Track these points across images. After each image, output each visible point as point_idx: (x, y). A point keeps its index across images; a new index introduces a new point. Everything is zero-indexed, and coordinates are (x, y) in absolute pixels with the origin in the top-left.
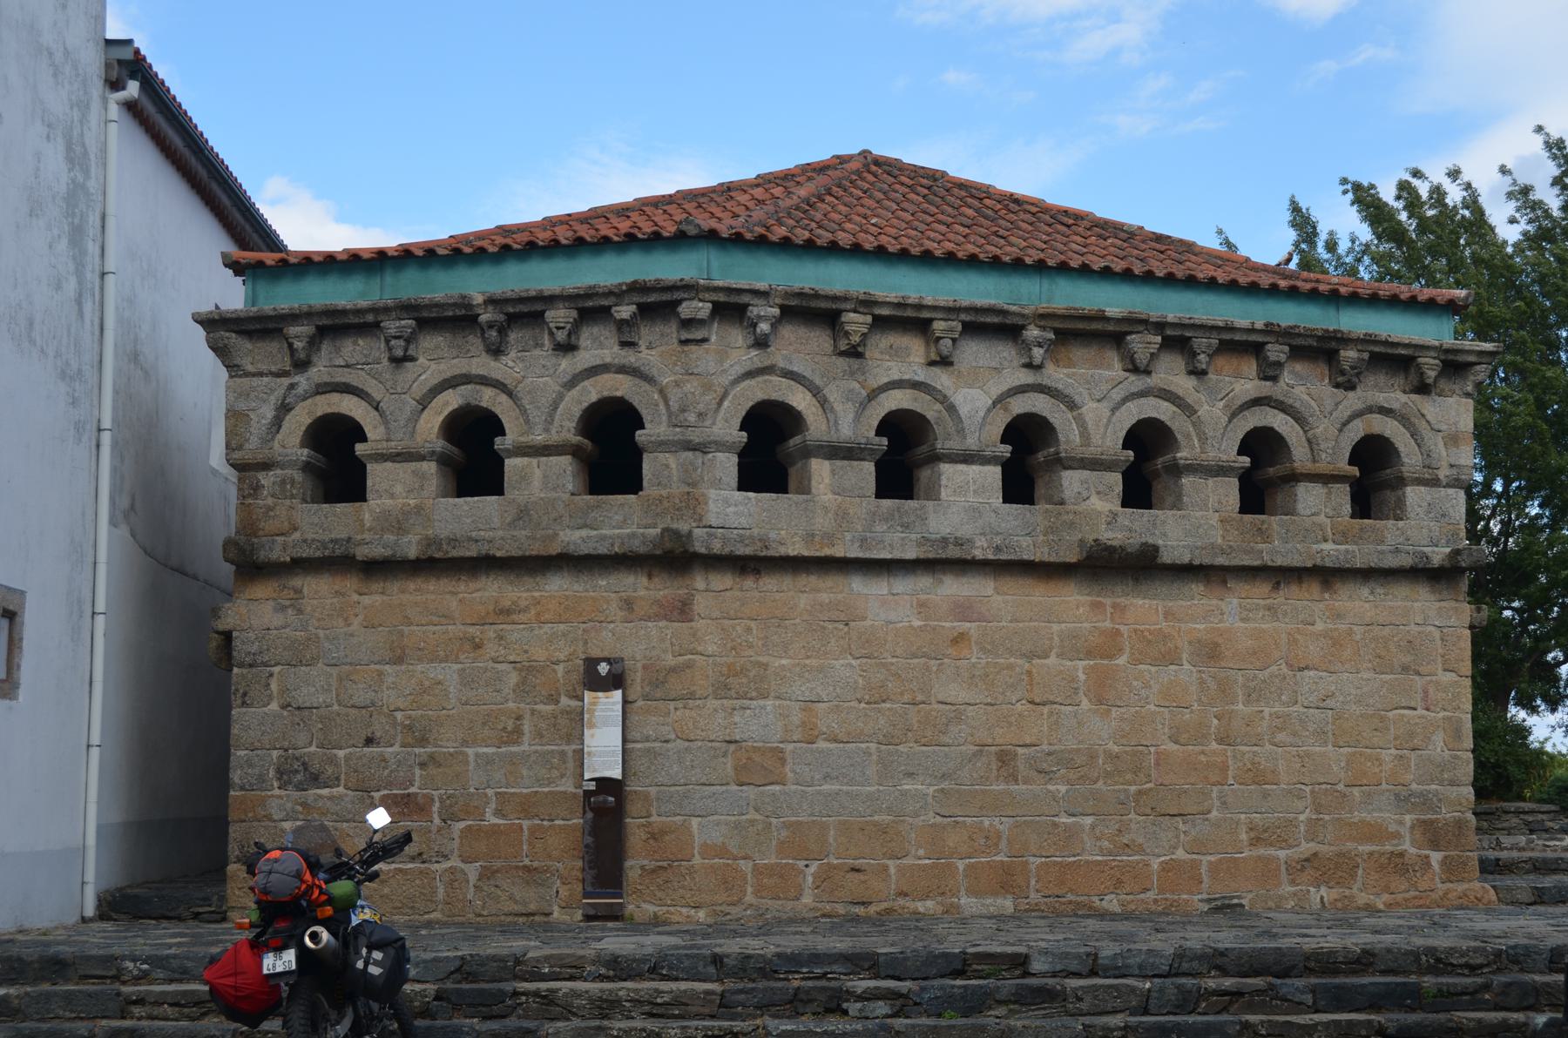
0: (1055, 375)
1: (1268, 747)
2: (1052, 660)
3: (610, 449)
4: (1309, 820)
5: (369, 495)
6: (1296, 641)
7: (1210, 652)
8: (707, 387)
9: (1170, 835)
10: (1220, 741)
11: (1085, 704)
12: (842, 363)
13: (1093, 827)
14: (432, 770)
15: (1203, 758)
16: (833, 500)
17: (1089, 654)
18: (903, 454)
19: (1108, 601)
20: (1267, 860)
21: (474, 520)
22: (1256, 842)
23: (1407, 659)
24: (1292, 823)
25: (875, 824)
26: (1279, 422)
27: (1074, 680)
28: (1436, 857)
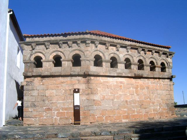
3: (77, 61)
5: (43, 67)
8: (90, 52)
14: (52, 104)
16: (105, 69)
18: (114, 63)
19: (137, 81)
21: (57, 70)
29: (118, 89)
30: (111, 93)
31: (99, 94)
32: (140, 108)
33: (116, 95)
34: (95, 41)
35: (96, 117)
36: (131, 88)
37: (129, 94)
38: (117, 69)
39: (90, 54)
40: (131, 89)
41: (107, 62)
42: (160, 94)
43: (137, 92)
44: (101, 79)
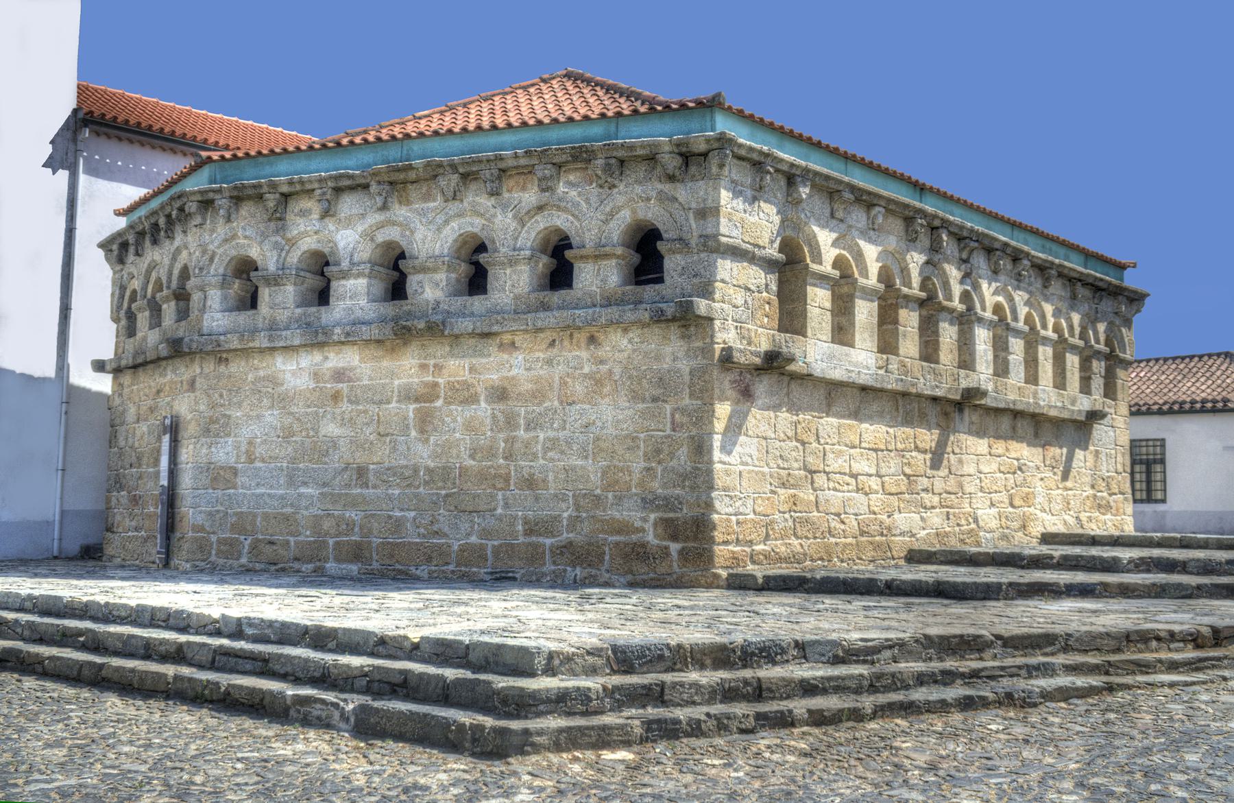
0: (400, 212)
1: (542, 462)
2: (394, 405)
4: (570, 516)
6: (566, 383)
7: (500, 394)
9: (467, 525)
10: (506, 458)
11: (413, 433)
13: (414, 519)
17: (417, 400)
20: (535, 546)
22: (529, 532)
23: (658, 392)
24: (557, 519)
25: (283, 514)
26: (561, 221)
28: (674, 547)
38: (323, 309)
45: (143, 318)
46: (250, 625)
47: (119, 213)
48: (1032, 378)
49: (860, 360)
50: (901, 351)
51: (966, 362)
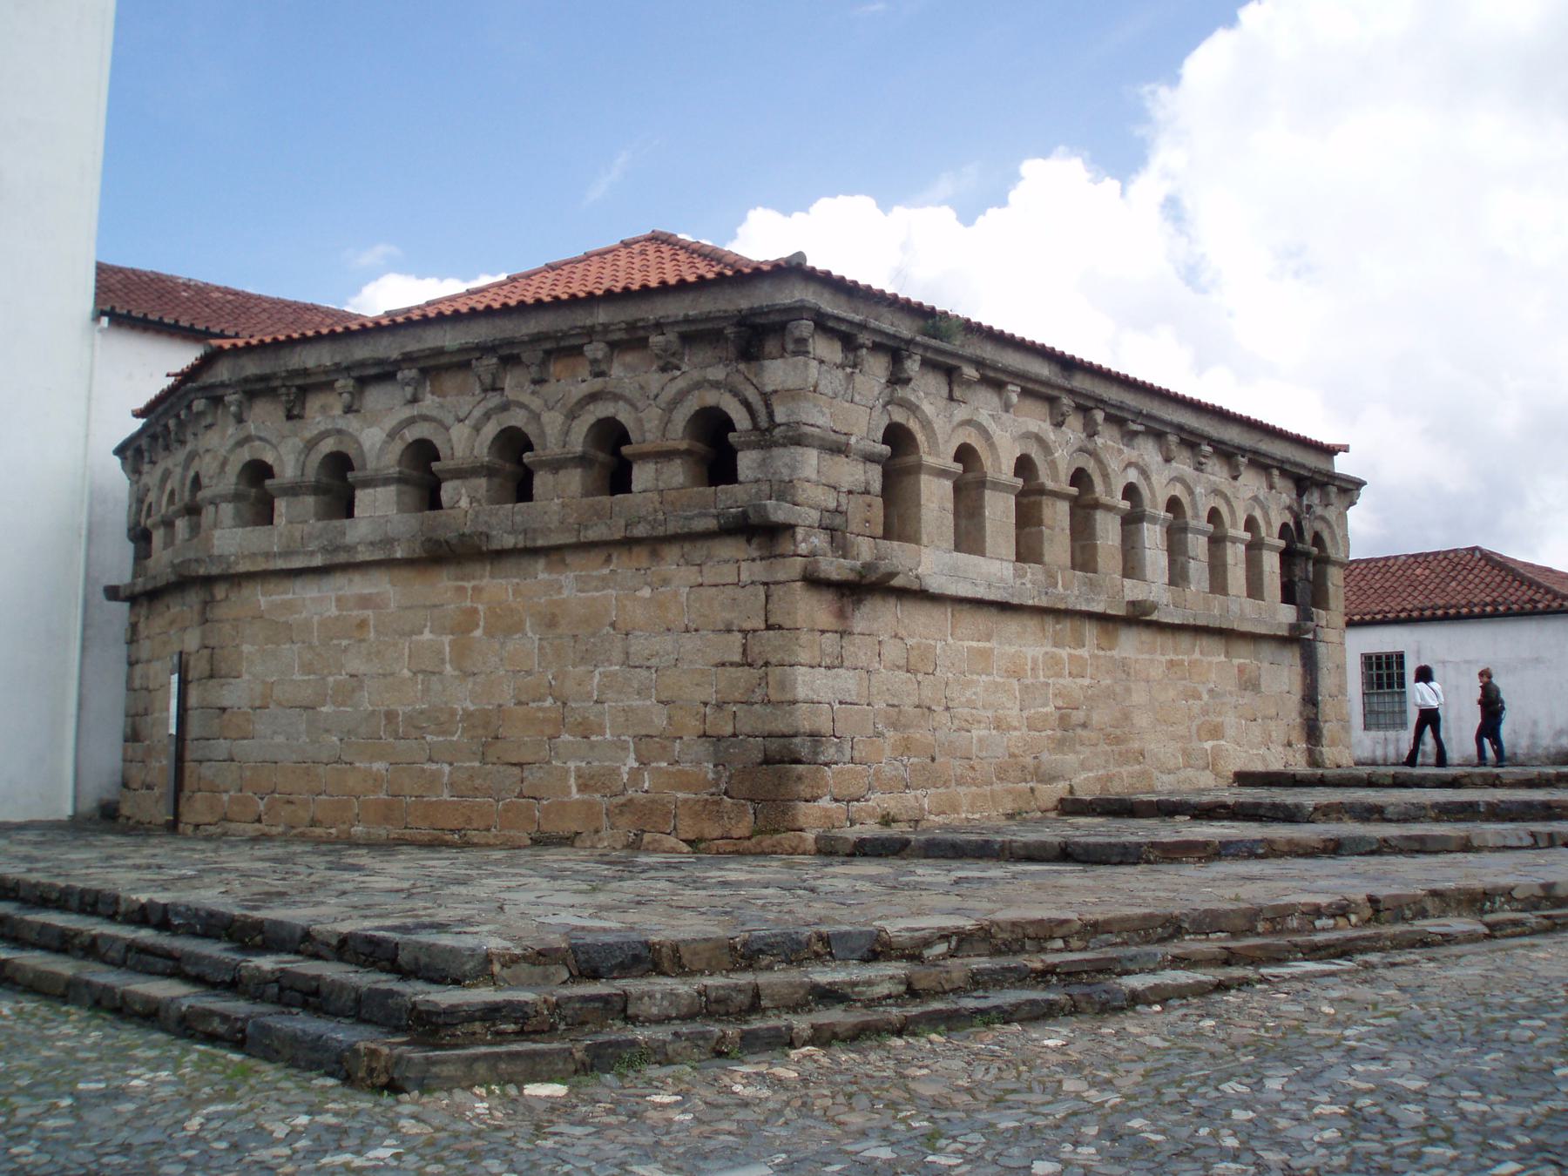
12: (289, 425)
15: (541, 715)
18: (338, 483)
19: (469, 585)
27: (440, 652)
29: (344, 643)
30: (307, 668)
31: (246, 677)
32: (477, 764)
33: (331, 679)
34: (219, 392)
35: (225, 797)
36: (427, 631)
37: (406, 673)
38: (347, 522)
39: (215, 465)
40: (427, 635)
41: (295, 494)
42: (653, 662)
43: (461, 652)
44: (263, 598)
45: (158, 537)
46: (177, 914)
47: (138, 414)
48: (1218, 584)
49: (993, 571)
50: (1047, 559)
51: (1132, 567)
